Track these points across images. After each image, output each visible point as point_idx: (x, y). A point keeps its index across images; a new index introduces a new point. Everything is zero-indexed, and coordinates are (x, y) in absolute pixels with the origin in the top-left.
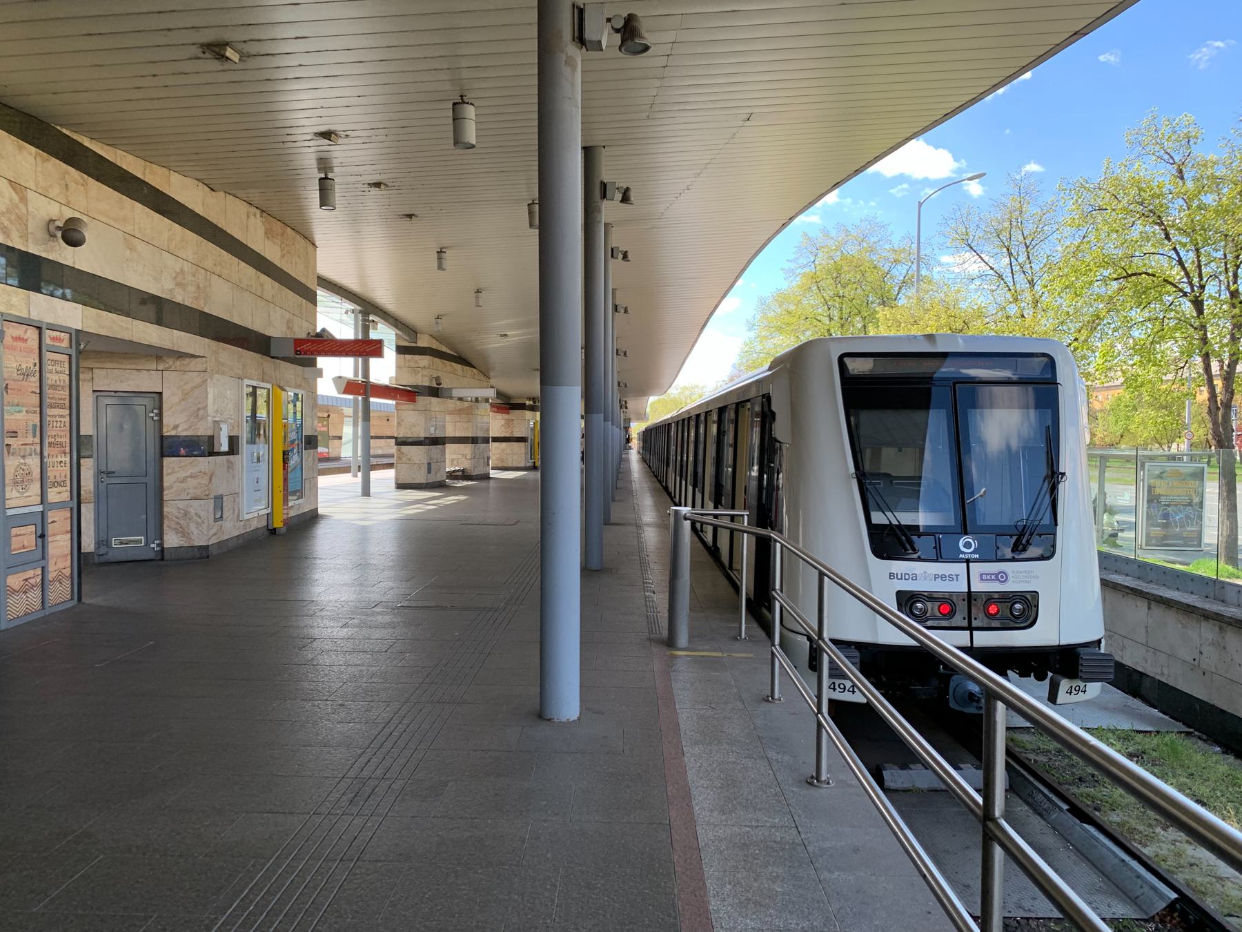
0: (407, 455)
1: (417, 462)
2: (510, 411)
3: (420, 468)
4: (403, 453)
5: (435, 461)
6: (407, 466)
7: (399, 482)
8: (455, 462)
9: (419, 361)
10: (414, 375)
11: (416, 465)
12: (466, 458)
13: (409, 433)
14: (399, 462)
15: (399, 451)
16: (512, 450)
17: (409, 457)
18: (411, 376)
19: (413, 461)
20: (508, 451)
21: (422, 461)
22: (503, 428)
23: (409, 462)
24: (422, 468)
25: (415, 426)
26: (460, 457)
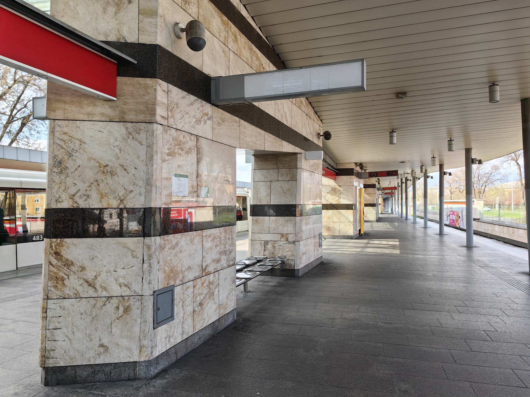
0: (83, 269)
1: (116, 290)
2: (337, 177)
3: (127, 310)
4: (68, 264)
5: (190, 275)
6: (83, 305)
7: (51, 363)
8: (270, 246)
10: (111, 10)
11: (115, 301)
12: (287, 240)
13: (94, 195)
14: (54, 293)
15: (57, 254)
16: (338, 218)
17: (90, 275)
18: (105, 10)
19: (105, 289)
20: (335, 219)
21: (136, 287)
23: (91, 292)
24: (135, 312)
25: (112, 174)
26: (277, 237)
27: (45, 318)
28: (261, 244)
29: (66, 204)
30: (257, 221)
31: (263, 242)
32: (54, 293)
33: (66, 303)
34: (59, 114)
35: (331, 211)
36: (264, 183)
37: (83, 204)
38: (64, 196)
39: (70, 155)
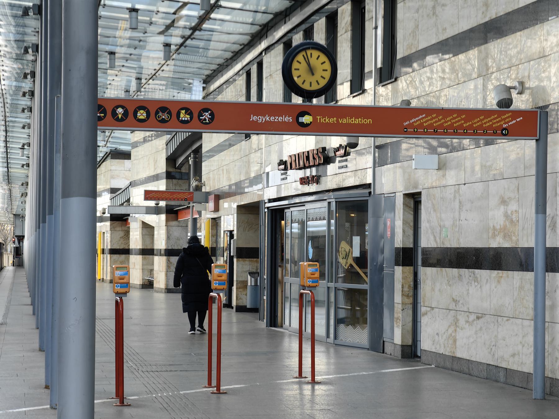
4: (171, 263)
7: (168, 288)
9: (182, 184)
13: (176, 245)
14: (169, 270)
15: (169, 260)
22: (122, 240)
25: (179, 240)
27: (167, 276)
28: (148, 271)
29: (170, 248)
30: (145, 258)
31: (149, 270)
32: (169, 270)
33: (171, 273)
34: (168, 224)
35: (124, 255)
36: (148, 236)
37: (174, 248)
38: (170, 246)
39: (171, 235)
